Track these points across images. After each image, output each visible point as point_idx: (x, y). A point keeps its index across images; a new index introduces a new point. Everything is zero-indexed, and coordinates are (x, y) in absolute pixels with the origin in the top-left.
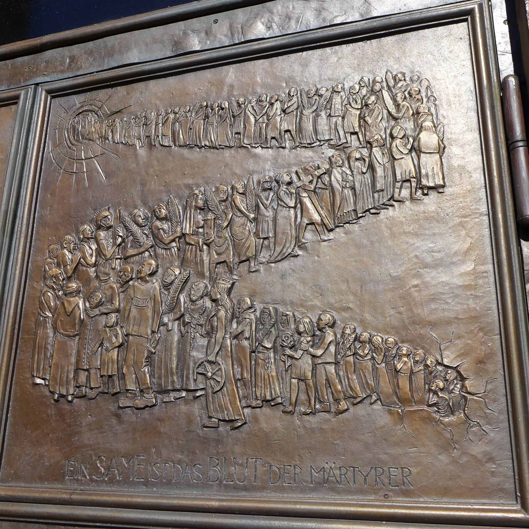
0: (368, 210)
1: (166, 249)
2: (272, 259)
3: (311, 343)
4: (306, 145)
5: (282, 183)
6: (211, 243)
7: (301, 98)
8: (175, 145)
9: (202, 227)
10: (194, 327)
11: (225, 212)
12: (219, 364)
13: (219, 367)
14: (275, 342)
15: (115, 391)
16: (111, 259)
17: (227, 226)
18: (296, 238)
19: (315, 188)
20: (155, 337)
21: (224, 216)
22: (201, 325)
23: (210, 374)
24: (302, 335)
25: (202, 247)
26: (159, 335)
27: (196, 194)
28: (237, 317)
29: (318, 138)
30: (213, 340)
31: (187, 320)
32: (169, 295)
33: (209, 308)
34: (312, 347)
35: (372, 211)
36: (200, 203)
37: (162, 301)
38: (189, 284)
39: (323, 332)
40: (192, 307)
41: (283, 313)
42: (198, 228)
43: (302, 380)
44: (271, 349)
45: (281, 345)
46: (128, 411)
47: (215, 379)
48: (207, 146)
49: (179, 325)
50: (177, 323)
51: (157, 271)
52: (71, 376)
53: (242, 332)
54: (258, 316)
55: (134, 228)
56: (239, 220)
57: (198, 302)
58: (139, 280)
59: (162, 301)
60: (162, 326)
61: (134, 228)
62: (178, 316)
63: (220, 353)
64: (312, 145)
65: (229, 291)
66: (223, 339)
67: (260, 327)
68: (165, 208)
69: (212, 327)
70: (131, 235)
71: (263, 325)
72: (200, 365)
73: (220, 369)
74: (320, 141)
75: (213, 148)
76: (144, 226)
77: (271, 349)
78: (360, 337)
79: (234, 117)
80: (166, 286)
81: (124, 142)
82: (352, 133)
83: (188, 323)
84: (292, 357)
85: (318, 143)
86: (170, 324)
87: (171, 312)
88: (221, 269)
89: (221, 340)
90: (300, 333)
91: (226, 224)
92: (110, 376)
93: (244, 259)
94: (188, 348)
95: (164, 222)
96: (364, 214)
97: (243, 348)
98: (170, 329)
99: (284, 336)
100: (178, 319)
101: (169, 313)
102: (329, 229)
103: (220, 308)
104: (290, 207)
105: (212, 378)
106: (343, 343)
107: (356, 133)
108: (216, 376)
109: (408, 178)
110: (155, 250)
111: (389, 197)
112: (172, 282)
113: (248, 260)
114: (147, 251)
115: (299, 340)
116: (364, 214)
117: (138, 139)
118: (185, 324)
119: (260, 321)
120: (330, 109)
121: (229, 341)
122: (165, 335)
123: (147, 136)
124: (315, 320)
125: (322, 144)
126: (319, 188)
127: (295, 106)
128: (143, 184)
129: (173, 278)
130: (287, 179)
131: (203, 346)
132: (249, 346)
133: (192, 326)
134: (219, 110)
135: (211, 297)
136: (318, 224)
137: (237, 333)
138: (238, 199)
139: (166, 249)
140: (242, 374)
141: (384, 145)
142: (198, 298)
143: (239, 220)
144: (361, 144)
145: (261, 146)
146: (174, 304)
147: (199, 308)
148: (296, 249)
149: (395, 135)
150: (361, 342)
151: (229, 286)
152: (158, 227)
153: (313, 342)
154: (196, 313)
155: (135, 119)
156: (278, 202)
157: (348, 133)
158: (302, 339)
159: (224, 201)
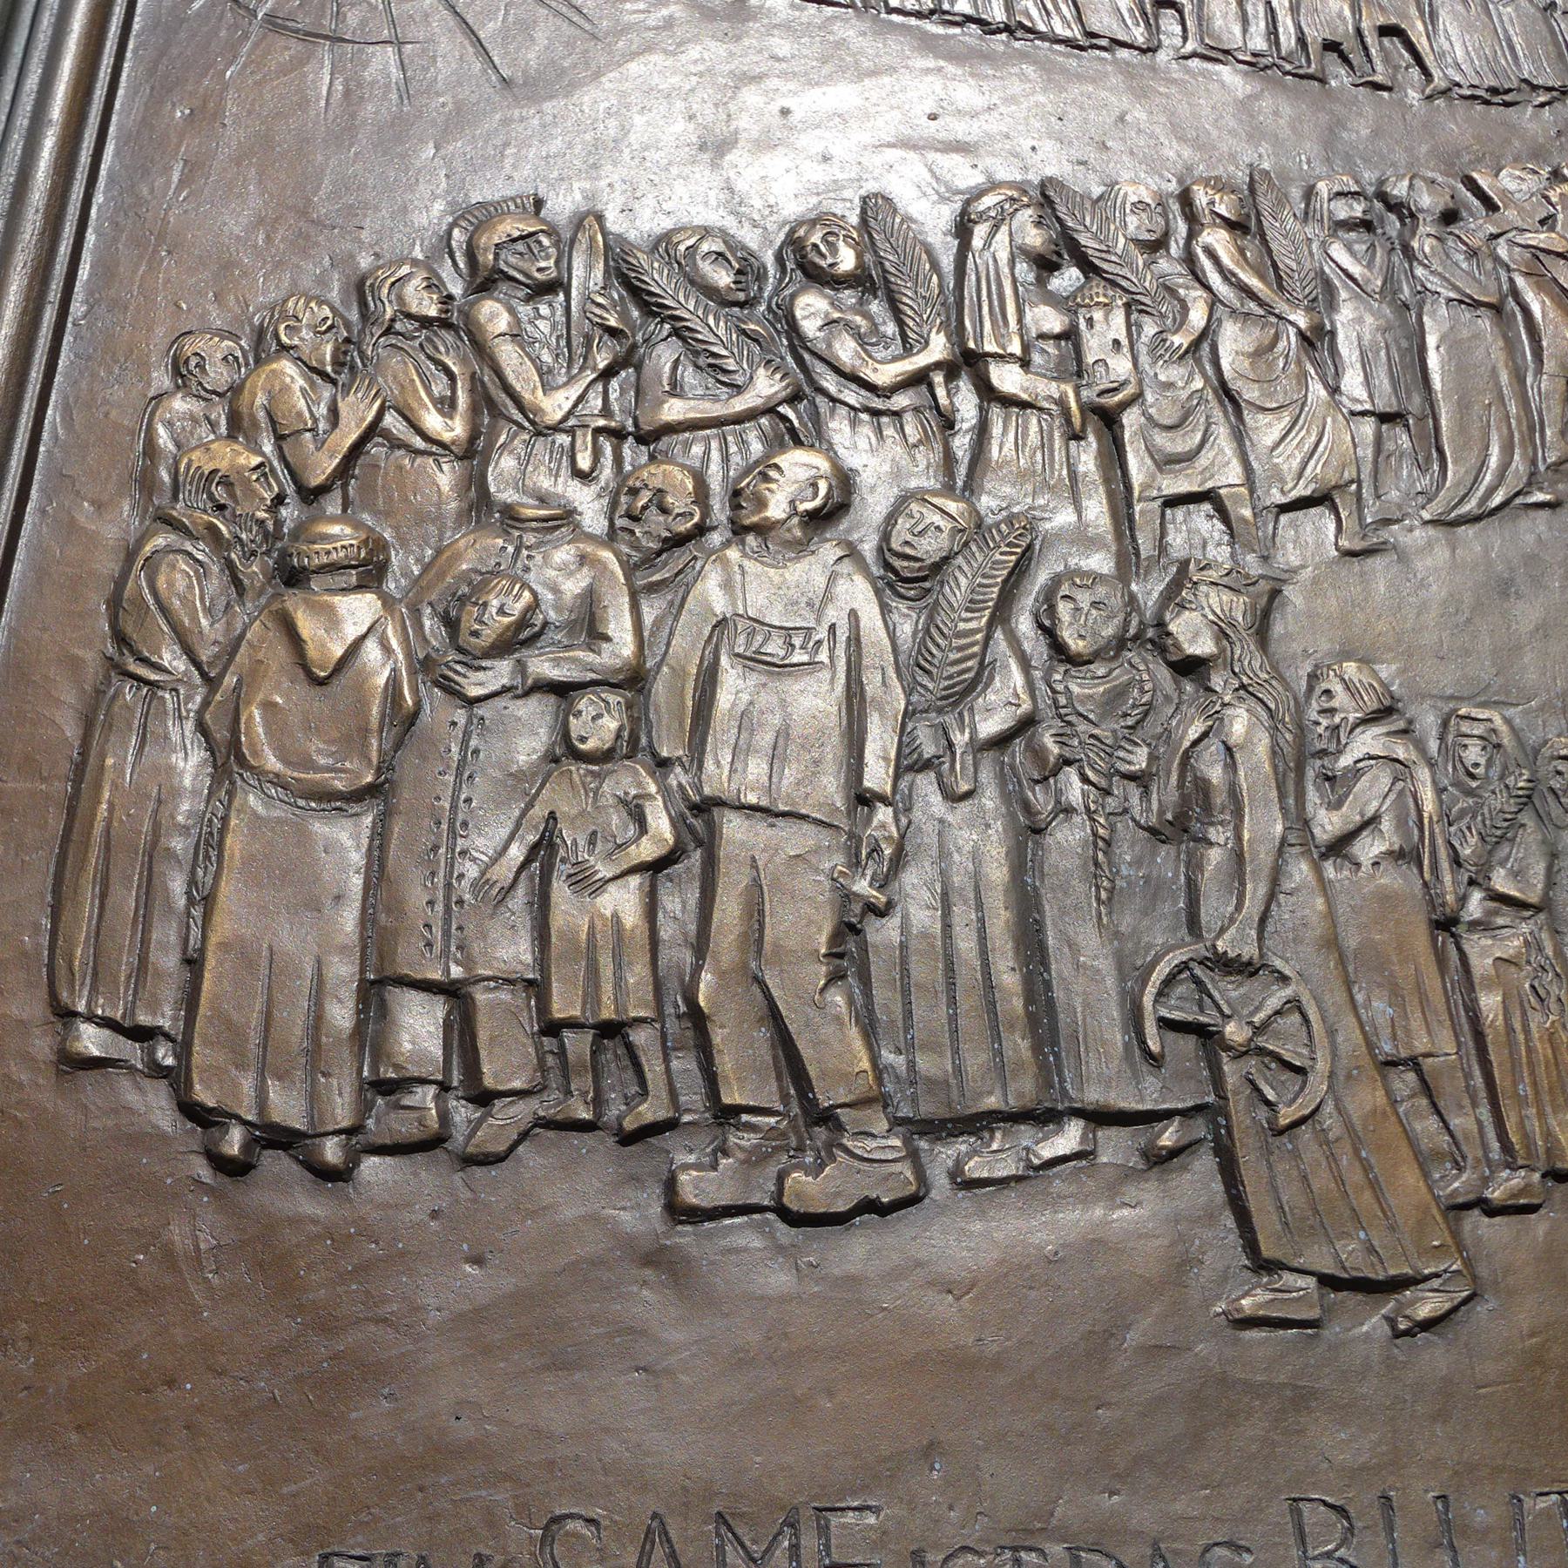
5: (1421, 210)
9: (1070, 335)
10: (1103, 783)
12: (1284, 979)
13: (1288, 992)
15: (650, 1111)
16: (571, 431)
17: (1196, 345)
23: (1234, 1032)
28: (1323, 753)
33: (1167, 698)
36: (1034, 238)
46: (743, 1235)
50: (987, 759)
52: (341, 1015)
53: (1371, 822)
58: (751, 540)
61: (688, 306)
64: (1507, 98)
69: (1203, 786)
70: (675, 332)
72: (1169, 981)
73: (1295, 1005)
74: (1535, 88)
76: (741, 305)
77: (1538, 909)
91: (1180, 340)
92: (611, 1031)
98: (964, 787)
100: (1001, 742)
105: (1250, 1050)
110: (816, 418)
112: (946, 560)
125: (1542, 99)
135: (1177, 646)
139: (876, 413)
154: (1103, 716)
159: (1156, 246)
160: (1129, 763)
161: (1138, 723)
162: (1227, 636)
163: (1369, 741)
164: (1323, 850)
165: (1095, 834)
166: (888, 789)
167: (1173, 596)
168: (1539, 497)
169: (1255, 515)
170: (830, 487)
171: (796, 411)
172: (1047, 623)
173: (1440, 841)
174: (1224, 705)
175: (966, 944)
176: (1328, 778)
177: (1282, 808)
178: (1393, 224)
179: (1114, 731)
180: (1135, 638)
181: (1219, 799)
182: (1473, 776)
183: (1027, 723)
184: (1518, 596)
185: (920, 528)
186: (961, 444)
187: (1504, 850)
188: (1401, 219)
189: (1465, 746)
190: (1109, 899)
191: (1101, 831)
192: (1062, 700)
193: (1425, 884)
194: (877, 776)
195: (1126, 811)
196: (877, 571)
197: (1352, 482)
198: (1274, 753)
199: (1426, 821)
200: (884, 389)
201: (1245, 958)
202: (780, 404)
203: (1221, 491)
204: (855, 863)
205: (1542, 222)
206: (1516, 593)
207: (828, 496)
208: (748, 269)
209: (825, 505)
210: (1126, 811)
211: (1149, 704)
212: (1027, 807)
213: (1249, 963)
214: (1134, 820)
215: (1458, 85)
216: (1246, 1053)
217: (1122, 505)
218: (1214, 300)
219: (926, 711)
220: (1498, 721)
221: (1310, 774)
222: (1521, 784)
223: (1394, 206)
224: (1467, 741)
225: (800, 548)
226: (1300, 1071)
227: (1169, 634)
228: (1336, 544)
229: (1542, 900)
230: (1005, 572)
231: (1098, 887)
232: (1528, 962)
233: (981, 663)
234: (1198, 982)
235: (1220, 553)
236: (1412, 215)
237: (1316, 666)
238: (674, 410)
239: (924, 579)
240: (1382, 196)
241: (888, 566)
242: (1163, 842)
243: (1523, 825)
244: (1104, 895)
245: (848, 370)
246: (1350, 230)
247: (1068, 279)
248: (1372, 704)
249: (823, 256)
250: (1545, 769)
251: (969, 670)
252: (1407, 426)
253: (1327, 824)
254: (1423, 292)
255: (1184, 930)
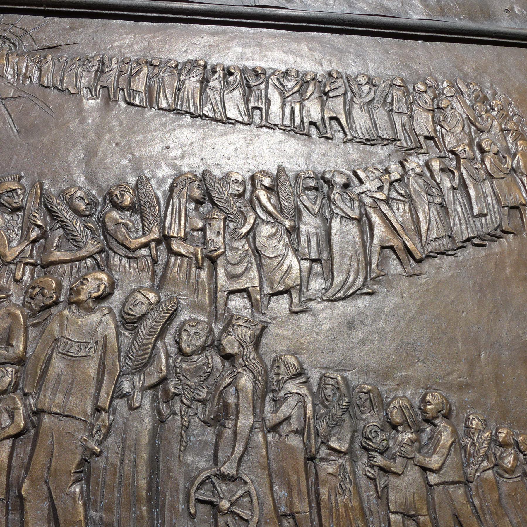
0: (469, 240)
1: (129, 258)
2: (329, 294)
3: (416, 444)
4: (364, 141)
5: (336, 184)
6: (219, 256)
7: (349, 83)
8: (151, 107)
9: (203, 230)
10: (189, 403)
11: (242, 213)
12: (245, 483)
13: (246, 488)
14: (352, 442)
16: (16, 264)
17: (248, 233)
18: (366, 265)
19: (388, 198)
20: (103, 421)
21: (240, 218)
22: (203, 402)
23: (225, 504)
24: (400, 429)
25: (203, 263)
26: (112, 417)
27: (190, 179)
28: (274, 391)
29: (380, 134)
30: (228, 432)
31: (173, 390)
32: (135, 339)
33: (218, 370)
34: (419, 451)
35: (475, 241)
36: (197, 193)
37: (119, 350)
38: (176, 324)
39: (435, 425)
40: (184, 366)
41: (362, 388)
42: (193, 230)
43: (410, 516)
44: (346, 453)
45: (364, 448)
47: (238, 515)
48: (207, 117)
49: (154, 399)
51: (110, 294)
53: (287, 419)
54: (315, 389)
55: (68, 216)
56: (266, 230)
57: (195, 358)
58: (73, 307)
59: (119, 350)
60: (118, 397)
61: (68, 216)
62: (153, 380)
63: (245, 458)
64: (372, 143)
65: (257, 342)
66: (251, 431)
67: (322, 411)
68: (131, 191)
69: (226, 405)
70: (62, 226)
71: (326, 407)
72: (202, 483)
73: (248, 493)
74: (383, 139)
75: (217, 121)
76: (88, 216)
77: (346, 453)
78: (497, 436)
79: (249, 87)
80: (129, 322)
81: (60, 87)
82: (426, 138)
83: (177, 395)
84: (384, 470)
85: (380, 141)
86: (137, 395)
87: (139, 372)
88: (238, 303)
89: (248, 432)
90: (395, 427)
91: (244, 231)
93: (281, 289)
94: (176, 446)
95: (128, 213)
96: (465, 244)
97: (290, 449)
98: (137, 405)
99: (368, 430)
100: (154, 386)
101: (133, 374)
102: (417, 258)
103: (240, 370)
104: (352, 218)
105: (229, 512)
106: (474, 444)
107: (432, 138)
108: (241, 507)
109: (516, 204)
110: (108, 258)
111: (496, 226)
112: (144, 315)
113: (287, 291)
114: (91, 256)
115: (395, 439)
116: (465, 244)
117: (86, 88)
118: (169, 398)
119: (320, 398)
120: (392, 103)
121: (260, 437)
122: (123, 417)
123: (102, 87)
124: (417, 402)
125: (385, 143)
126: (393, 199)
127: (341, 91)
128: (91, 153)
129: (144, 309)
130: (339, 180)
131: (206, 444)
132: (301, 445)
133: (185, 401)
134: (225, 75)
135: (224, 349)
136: (400, 250)
137: (278, 421)
138: (262, 195)
139: (129, 258)
140: (290, 504)
141: (473, 159)
142: (197, 350)
143: (266, 230)
144: (440, 152)
145: (294, 131)
146: (147, 356)
147: (200, 368)
148: (367, 283)
149: (486, 149)
150: (501, 445)
151: (258, 332)
152: (117, 220)
153: (420, 442)
154: (192, 377)
155: (84, 62)
156: (332, 210)
157: (422, 135)
158: (400, 437)
160: (200, 395)
161: (205, 379)
162: (242, 346)
163: (292, 387)
164: (269, 429)
165: (182, 424)
166: (107, 407)
167: (225, 330)
168: (365, 290)
169: (261, 298)
170: (105, 287)
171: (101, 257)
172: (177, 339)
173: (312, 426)
174: (238, 373)
175: (128, 469)
176: (274, 401)
177: (254, 413)
178: (326, 188)
179: (195, 383)
180: (209, 346)
181: (232, 410)
182: (327, 400)
183: (164, 380)
184: (355, 328)
185: (136, 303)
186: (159, 270)
187: (336, 429)
188: (329, 186)
189: (326, 388)
190: (184, 450)
191: (185, 423)
192: (178, 370)
193: (304, 444)
194: (104, 400)
195: (196, 414)
196: (118, 319)
197: (298, 285)
198: (253, 392)
199: (307, 418)
200: (132, 249)
201: (231, 475)
202: (95, 254)
203: (250, 289)
204: (91, 436)
205: (378, 188)
206: (354, 327)
207: (103, 291)
208: (92, 203)
209: (102, 294)
210: (196, 414)
211: (211, 372)
212: (160, 413)
213: (232, 477)
214: (198, 418)
215: (356, 138)
216: (227, 513)
217: (213, 294)
218: (257, 216)
219: (128, 374)
220: (339, 378)
221: (268, 399)
222: (344, 404)
223: (328, 182)
224: (327, 386)
225: (90, 311)
226: (247, 521)
227: (221, 345)
228: (290, 309)
229: (347, 450)
230: (164, 321)
231: (181, 445)
232: (340, 475)
233: (150, 356)
234: (213, 484)
235: (247, 313)
236: (332, 185)
237: (276, 356)
238: (58, 255)
239: (135, 322)
240: (323, 178)
241: (123, 317)
242: (209, 426)
243: (344, 420)
244: (182, 448)
245: (120, 242)
246: (310, 191)
247: (207, 206)
248: (293, 372)
249: (118, 199)
250: (355, 397)
251: (145, 358)
252: (321, 263)
253: (271, 418)
254: (332, 213)
255: (212, 462)
